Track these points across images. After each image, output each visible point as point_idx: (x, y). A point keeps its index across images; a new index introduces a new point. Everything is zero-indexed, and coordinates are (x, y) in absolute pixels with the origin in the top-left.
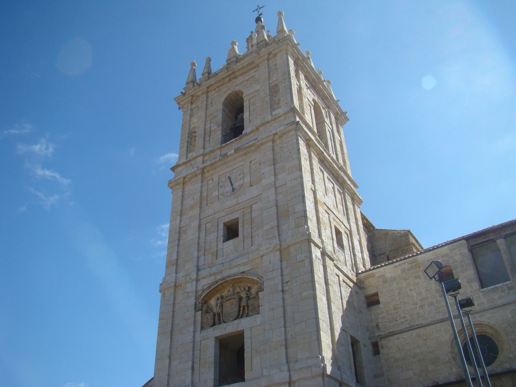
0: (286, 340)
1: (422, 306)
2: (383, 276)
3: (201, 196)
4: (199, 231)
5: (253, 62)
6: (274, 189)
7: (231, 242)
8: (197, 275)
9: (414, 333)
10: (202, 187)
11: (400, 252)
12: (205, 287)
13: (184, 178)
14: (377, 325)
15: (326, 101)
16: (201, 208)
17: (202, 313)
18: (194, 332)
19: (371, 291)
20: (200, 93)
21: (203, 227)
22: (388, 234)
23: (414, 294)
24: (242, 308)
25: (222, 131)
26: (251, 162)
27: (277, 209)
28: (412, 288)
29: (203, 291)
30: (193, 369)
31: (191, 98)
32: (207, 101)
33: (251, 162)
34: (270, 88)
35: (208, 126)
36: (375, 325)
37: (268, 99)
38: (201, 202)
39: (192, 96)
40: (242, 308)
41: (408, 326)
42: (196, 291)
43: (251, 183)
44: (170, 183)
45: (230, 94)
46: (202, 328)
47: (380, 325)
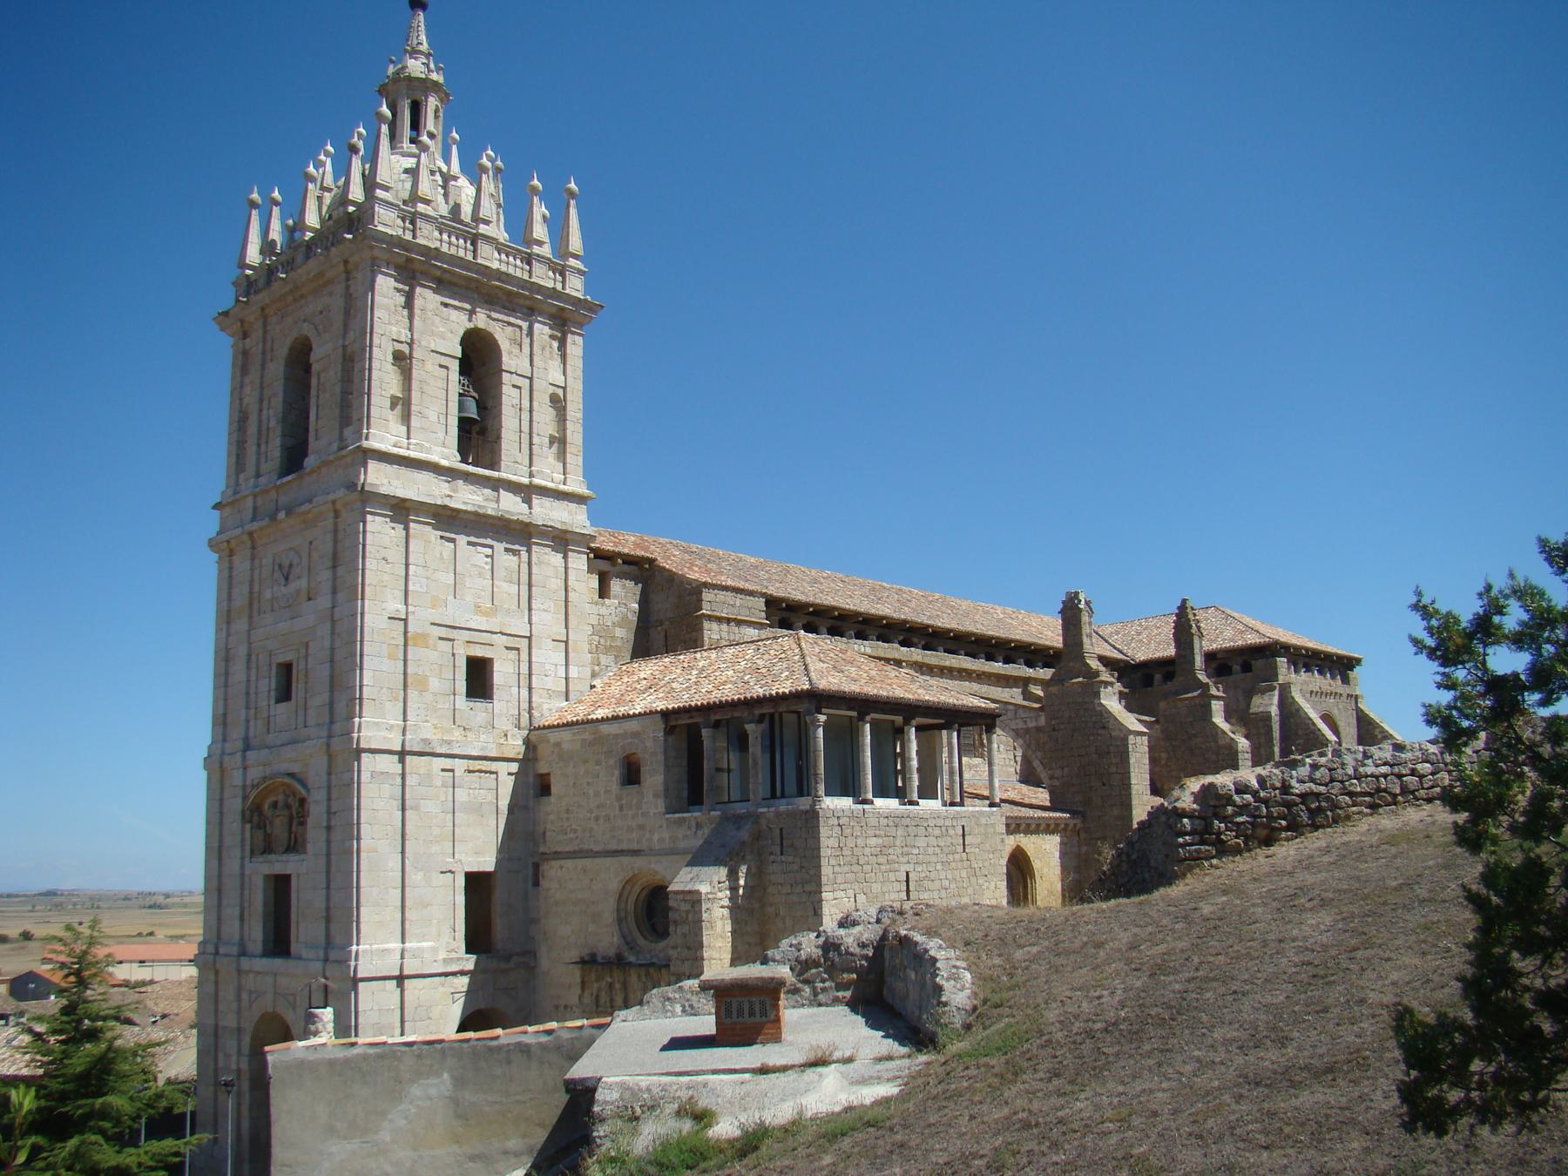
0: (328, 909)
1: (597, 818)
2: (558, 744)
3: (251, 592)
4: (248, 668)
5: (321, 274)
6: (329, 625)
7: (283, 705)
8: (244, 758)
9: (581, 863)
10: (252, 570)
11: (684, 628)
12: (256, 782)
13: (228, 542)
14: (544, 833)
15: (521, 301)
16: (251, 617)
17: (252, 828)
18: (243, 858)
19: (543, 768)
20: (252, 318)
21: (254, 658)
22: (673, 580)
23: (591, 792)
24: (293, 836)
25: (283, 436)
26: (311, 543)
27: (332, 669)
28: (590, 780)
29: (253, 786)
30: (242, 918)
31: (239, 324)
32: (264, 342)
33: (311, 543)
34: (344, 359)
35: (265, 412)
36: (542, 831)
37: (338, 389)
38: (251, 604)
39: (242, 321)
40: (293, 836)
41: (577, 849)
42: (244, 786)
43: (309, 592)
44: (210, 541)
45: (297, 339)
46: (252, 852)
47: (548, 834)
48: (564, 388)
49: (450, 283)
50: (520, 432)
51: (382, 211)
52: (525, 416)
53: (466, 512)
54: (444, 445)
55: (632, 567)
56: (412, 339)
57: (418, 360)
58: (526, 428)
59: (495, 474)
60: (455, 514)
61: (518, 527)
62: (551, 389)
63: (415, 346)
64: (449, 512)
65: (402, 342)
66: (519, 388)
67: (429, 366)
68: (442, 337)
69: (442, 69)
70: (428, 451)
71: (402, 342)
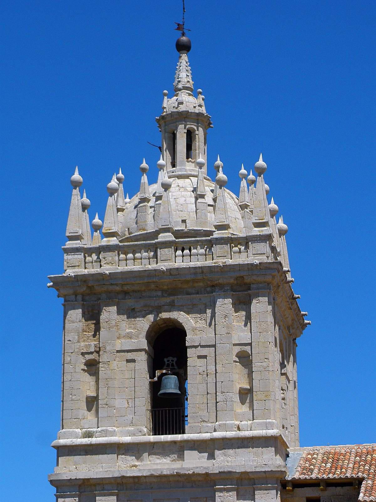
48: (250, 344)
49: (134, 291)
50: (208, 393)
51: (70, 257)
52: (211, 379)
53: (145, 477)
54: (132, 424)
55: (346, 488)
56: (100, 348)
57: (104, 363)
58: (212, 390)
59: (178, 437)
60: (136, 480)
61: (200, 478)
62: (237, 349)
63: (101, 353)
64: (131, 480)
65: (91, 353)
66: (205, 357)
67: (114, 365)
68: (129, 336)
69: (200, 93)
70: (113, 434)
71: (91, 353)
